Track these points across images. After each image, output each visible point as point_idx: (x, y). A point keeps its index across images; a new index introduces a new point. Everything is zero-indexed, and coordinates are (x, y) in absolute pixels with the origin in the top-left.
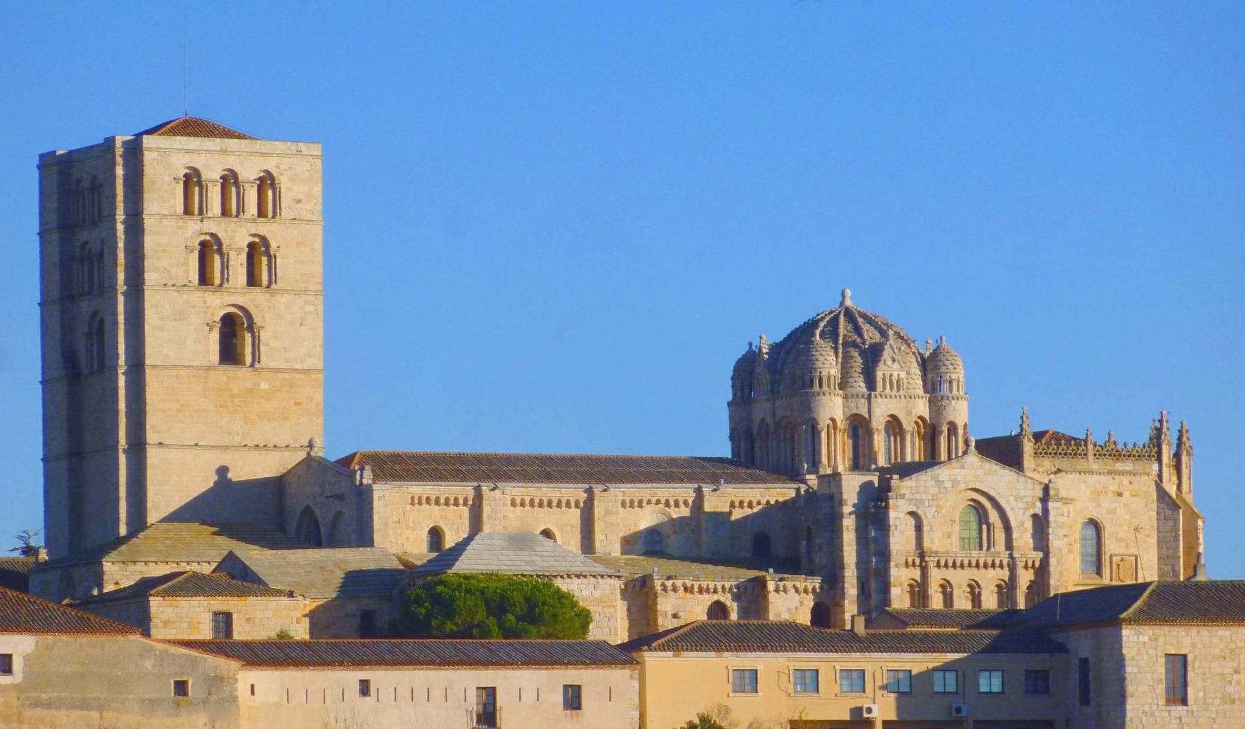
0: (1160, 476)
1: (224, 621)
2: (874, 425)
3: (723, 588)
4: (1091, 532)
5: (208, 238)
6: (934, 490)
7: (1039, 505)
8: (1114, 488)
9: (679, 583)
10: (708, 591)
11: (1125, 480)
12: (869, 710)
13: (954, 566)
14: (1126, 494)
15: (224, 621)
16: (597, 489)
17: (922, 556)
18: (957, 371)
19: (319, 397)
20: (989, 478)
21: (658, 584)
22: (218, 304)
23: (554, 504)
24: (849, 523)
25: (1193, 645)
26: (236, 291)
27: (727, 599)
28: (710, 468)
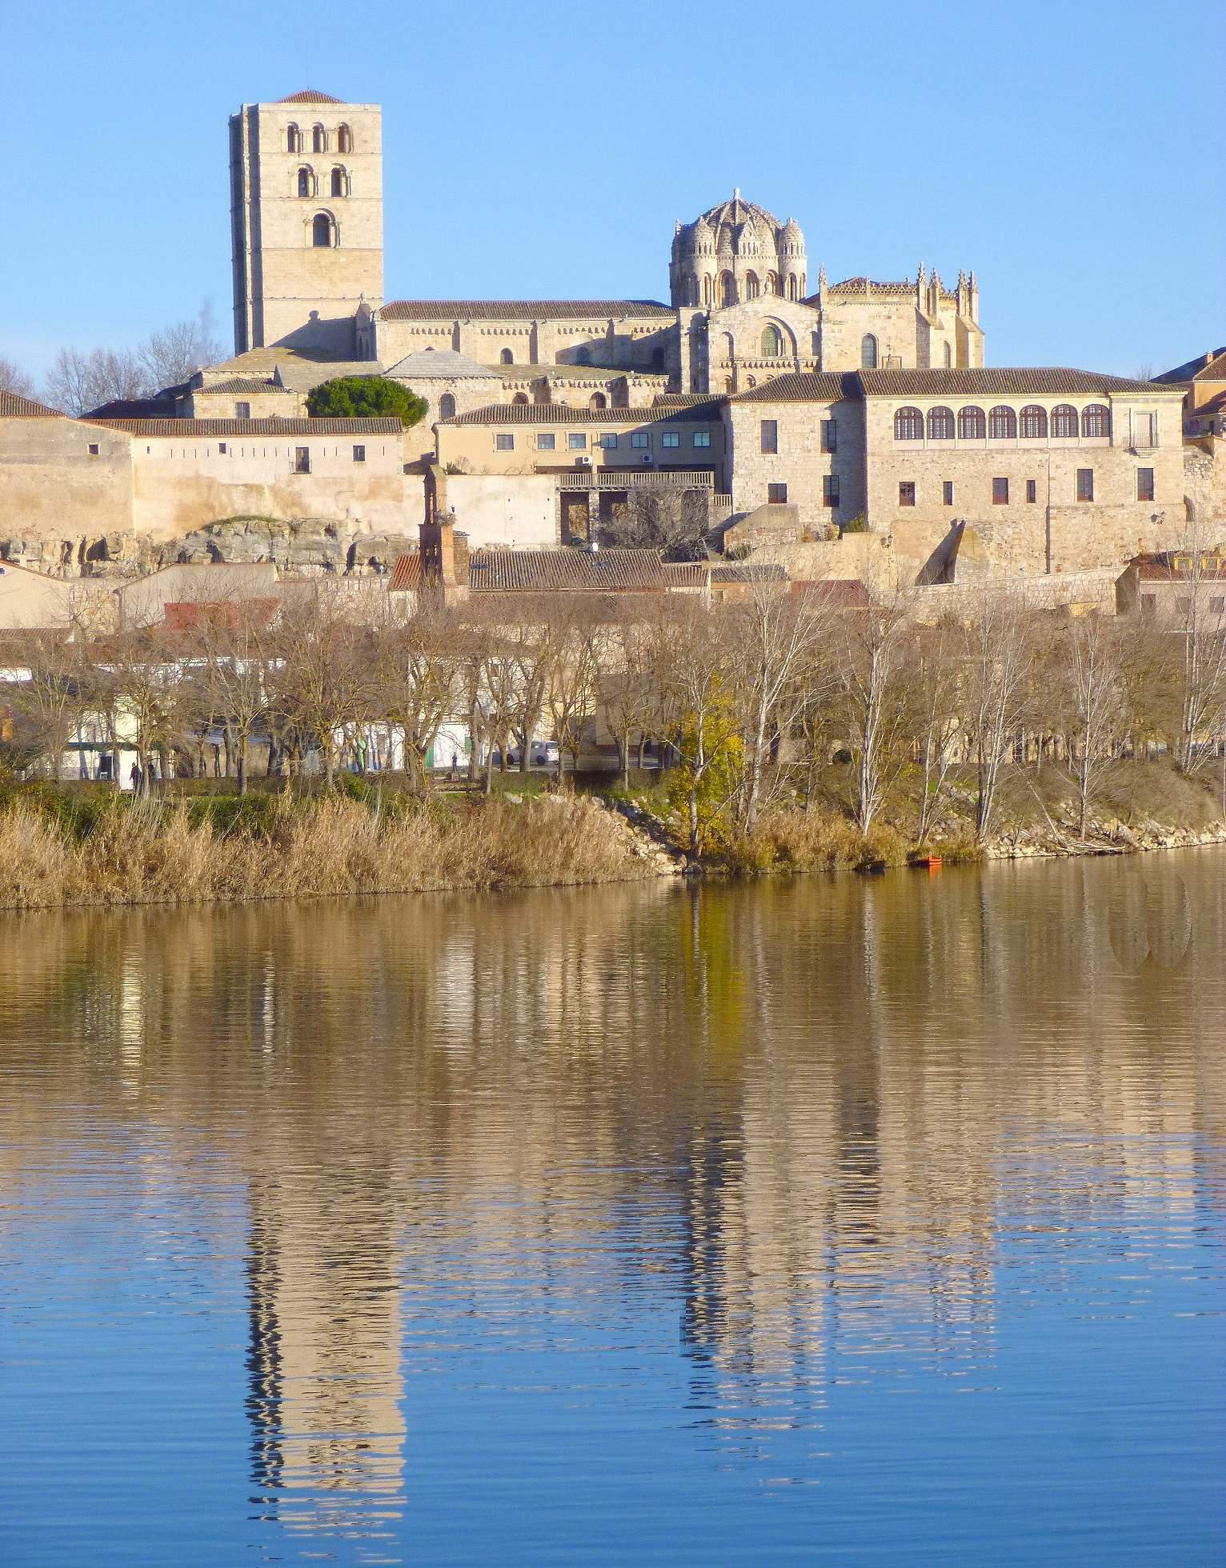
0: (918, 305)
1: (244, 408)
2: (737, 276)
3: (601, 383)
4: (869, 343)
5: (304, 167)
7: (815, 326)
8: (886, 313)
9: (566, 381)
10: (590, 386)
12: (587, 459)
13: (756, 366)
14: (894, 317)
15: (244, 408)
16: (539, 322)
17: (732, 360)
18: (798, 239)
19: (381, 267)
20: (780, 309)
21: (551, 384)
22: (311, 209)
23: (568, 331)
24: (685, 340)
25: (781, 415)
27: (527, 391)
28: (632, 307)
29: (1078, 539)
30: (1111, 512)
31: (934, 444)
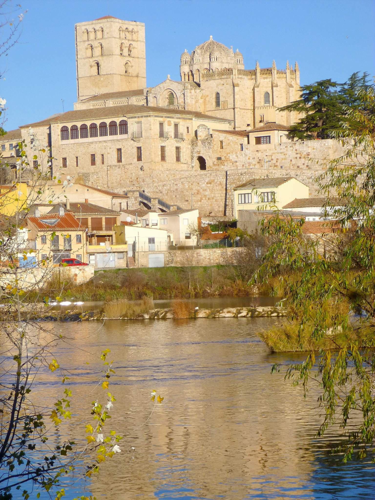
6: (159, 90)
8: (222, 83)
11: (225, 80)
14: (225, 84)
29: (117, 179)
30: (127, 167)
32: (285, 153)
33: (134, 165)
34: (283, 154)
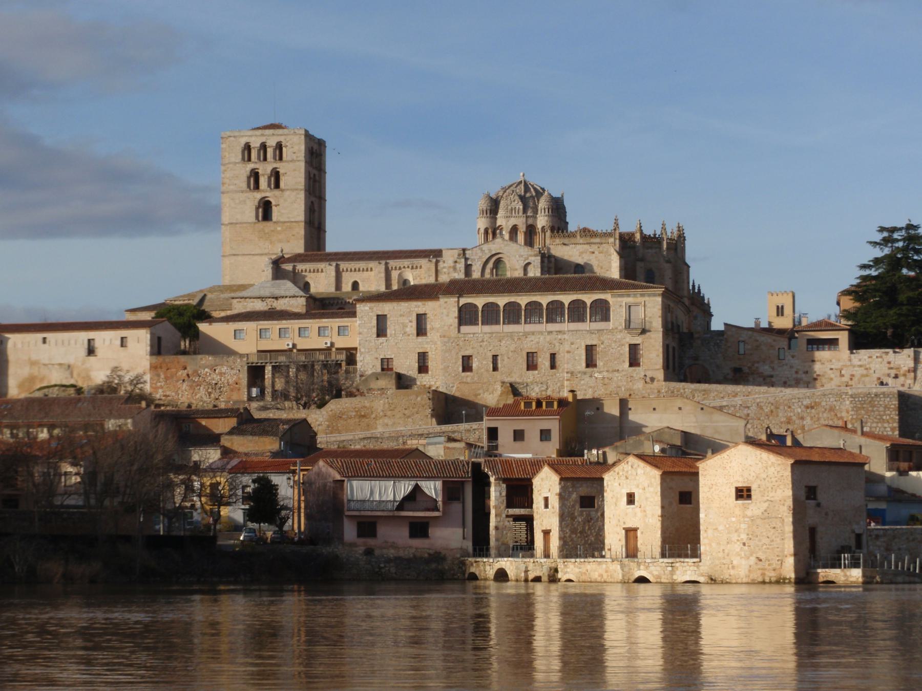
6: (480, 254)
14: (596, 252)
26: (263, 191)
31: (487, 328)
32: (868, 366)
33: (624, 373)
34: (863, 368)
